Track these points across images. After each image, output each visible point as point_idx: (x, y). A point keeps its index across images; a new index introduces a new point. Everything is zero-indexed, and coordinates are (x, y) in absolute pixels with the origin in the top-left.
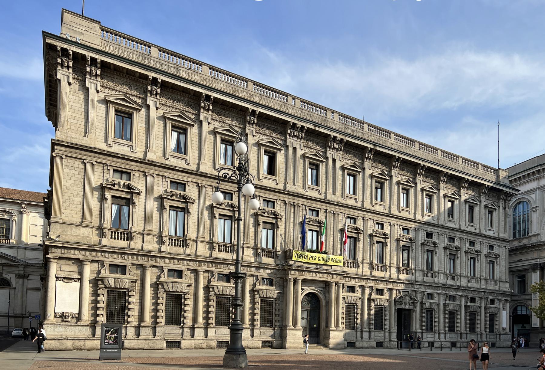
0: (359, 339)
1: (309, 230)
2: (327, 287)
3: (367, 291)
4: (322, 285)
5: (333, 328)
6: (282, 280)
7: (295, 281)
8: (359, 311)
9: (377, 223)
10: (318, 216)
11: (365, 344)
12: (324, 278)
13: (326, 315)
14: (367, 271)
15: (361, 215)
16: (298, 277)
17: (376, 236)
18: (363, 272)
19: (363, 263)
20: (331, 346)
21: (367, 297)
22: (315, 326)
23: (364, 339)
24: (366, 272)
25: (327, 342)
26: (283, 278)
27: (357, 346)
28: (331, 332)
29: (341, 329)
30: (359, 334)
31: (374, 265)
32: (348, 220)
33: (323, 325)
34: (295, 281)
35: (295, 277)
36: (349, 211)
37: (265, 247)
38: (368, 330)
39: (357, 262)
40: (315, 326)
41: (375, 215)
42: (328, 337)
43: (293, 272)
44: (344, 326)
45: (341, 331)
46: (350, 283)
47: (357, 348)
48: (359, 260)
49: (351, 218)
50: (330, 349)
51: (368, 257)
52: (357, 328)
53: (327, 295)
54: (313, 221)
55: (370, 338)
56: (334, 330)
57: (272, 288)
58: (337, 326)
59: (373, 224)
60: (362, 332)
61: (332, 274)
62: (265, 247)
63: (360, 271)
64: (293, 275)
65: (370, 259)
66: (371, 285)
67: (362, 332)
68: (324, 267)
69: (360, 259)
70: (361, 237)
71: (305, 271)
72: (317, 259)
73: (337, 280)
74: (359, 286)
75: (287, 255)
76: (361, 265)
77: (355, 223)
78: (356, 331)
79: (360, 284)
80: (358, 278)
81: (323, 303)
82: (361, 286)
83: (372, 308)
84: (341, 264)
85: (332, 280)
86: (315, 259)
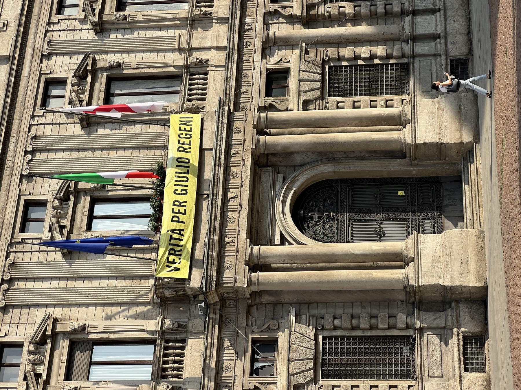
0: (440, 45)
1: (89, 227)
2: (272, 159)
3: (280, 29)
4: (267, 176)
5: (405, 135)
6: (254, 310)
7: (256, 265)
8: (347, 52)
9: (59, 12)
10: (42, 203)
11: (456, 25)
12: (243, 172)
13: (363, 158)
14: (217, 35)
15: (36, 63)
16: (243, 258)
17: (102, 11)
18: (218, 48)
19: (191, 50)
20: (467, 138)
21: (298, 31)
22: (401, 193)
23: (440, 30)
24: (218, 36)
25: (453, 152)
26: (249, 307)
27: (464, 50)
28: (420, 140)
29: (408, 108)
30: (422, 48)
31: (196, 11)
32: (54, 104)
33: (396, 167)
34: (256, 265)
35: (243, 268)
36: (24, 103)
37: (149, 368)
38: (407, 19)
39: (187, 67)
40: (401, 193)
41: (34, 18)
42: (438, 150)
43: (228, 275)
44: (397, 98)
45: (414, 108)
46: (256, 87)
47: (470, 51)
48: (180, 63)
49: (46, 97)
50: (477, 138)
51: (171, 33)
52: (403, 56)
53: (298, 159)
54: (59, 217)
55: (433, 11)
56: (414, 131)
57: (283, 338)
58: (398, 122)
59: (63, 25)
60: (414, 39)
61: (229, 146)
62: (149, 368)
63: (216, 58)
64: (236, 275)
65: (175, 27)
66: (260, 19)
67: (414, 39)
68: (208, 174)
69: (178, 59)
70: (105, 60)
71: (222, 236)
72: (181, 198)
73: (250, 128)
74: (264, 56)
75: (171, 297)
76: (196, 55)
77: (61, 82)
78: (414, 57)
79: (259, 54)
80: (240, 61)
81: (326, 170)
82: (264, 50)
83: (334, 12)
84: (197, 118)
85: (249, 145)
86: (181, 204)
